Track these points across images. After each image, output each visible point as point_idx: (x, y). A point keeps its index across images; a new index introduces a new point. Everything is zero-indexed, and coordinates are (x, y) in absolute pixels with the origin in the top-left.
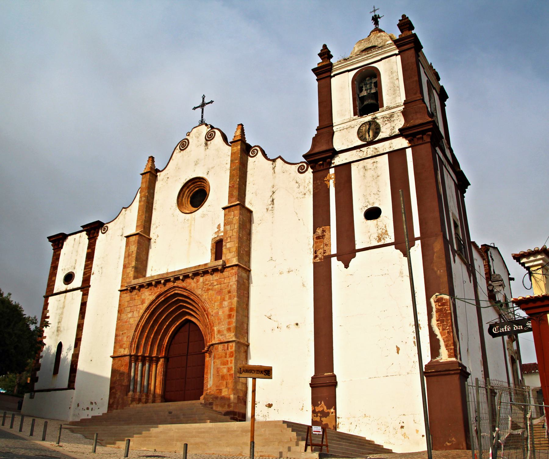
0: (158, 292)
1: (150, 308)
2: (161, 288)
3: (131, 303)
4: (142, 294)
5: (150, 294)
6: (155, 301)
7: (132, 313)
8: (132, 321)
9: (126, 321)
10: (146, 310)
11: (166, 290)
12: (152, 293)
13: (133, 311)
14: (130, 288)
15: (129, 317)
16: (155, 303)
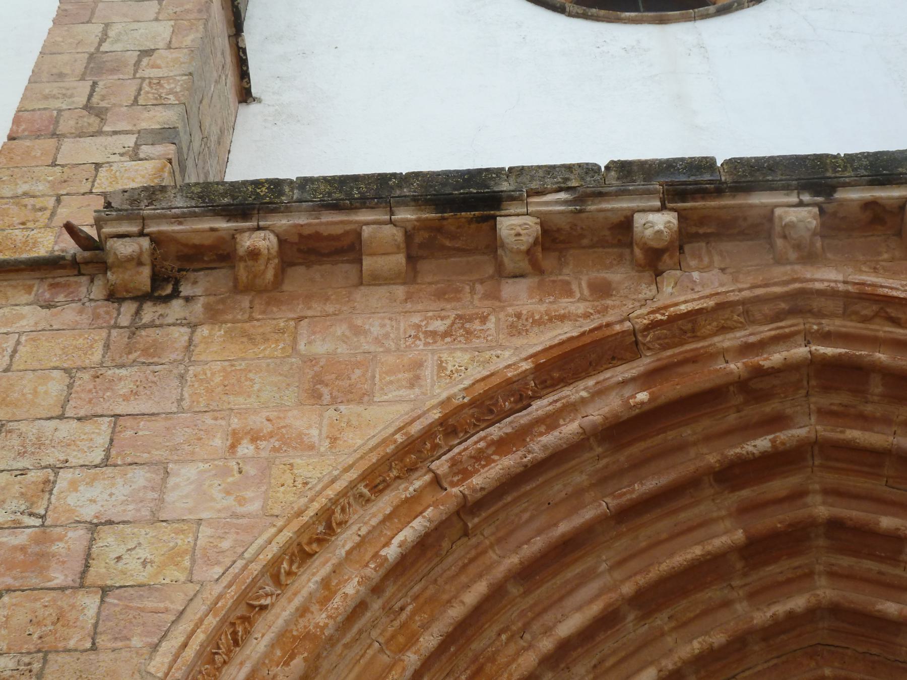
0: (562, 318)
1: (441, 466)
2: (602, 290)
3: (123, 388)
4: (301, 319)
5: (439, 326)
6: (523, 401)
7: (140, 477)
8: (143, 553)
9: (23, 549)
10: (386, 462)
11: (683, 308)
12: (476, 325)
13: (158, 455)
14: (145, 243)
15: (88, 513)
16: (523, 418)
